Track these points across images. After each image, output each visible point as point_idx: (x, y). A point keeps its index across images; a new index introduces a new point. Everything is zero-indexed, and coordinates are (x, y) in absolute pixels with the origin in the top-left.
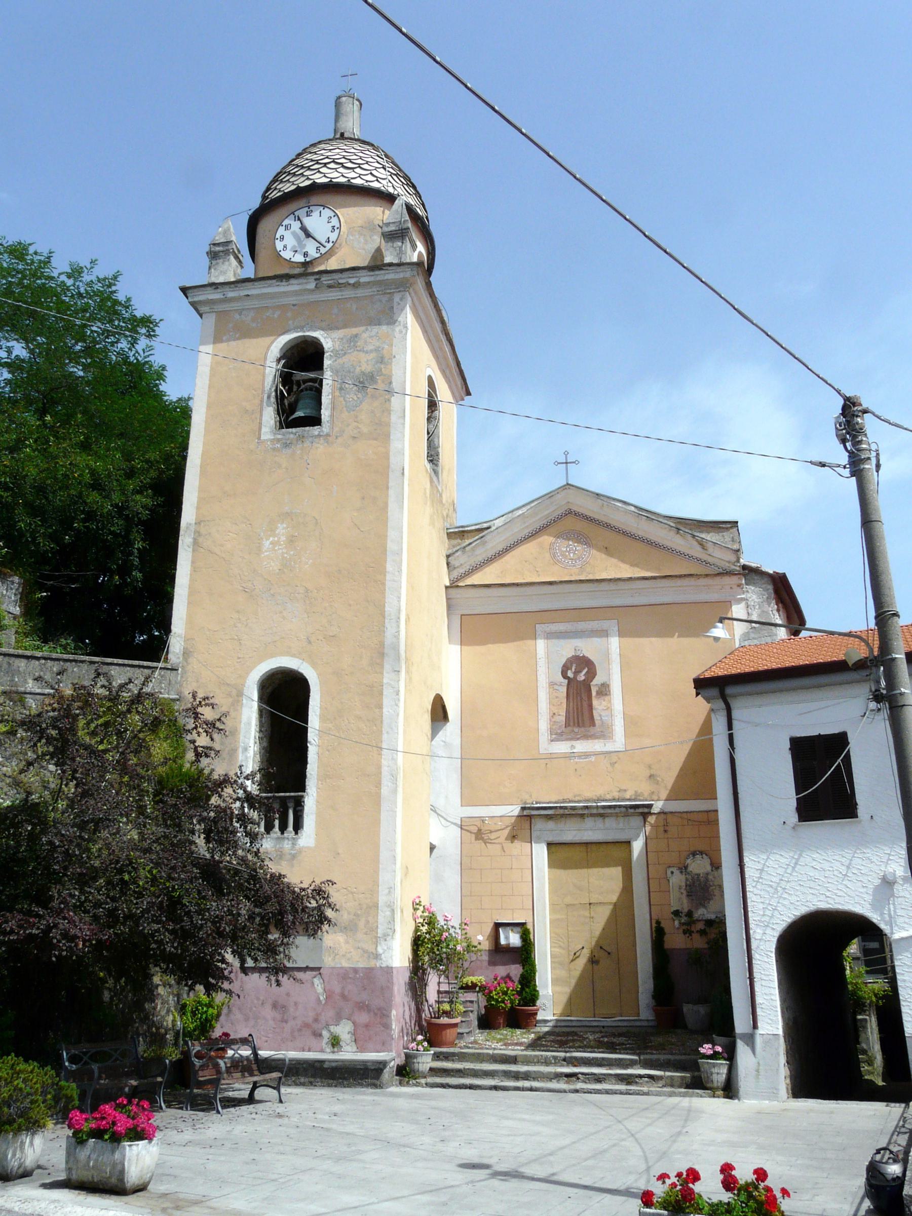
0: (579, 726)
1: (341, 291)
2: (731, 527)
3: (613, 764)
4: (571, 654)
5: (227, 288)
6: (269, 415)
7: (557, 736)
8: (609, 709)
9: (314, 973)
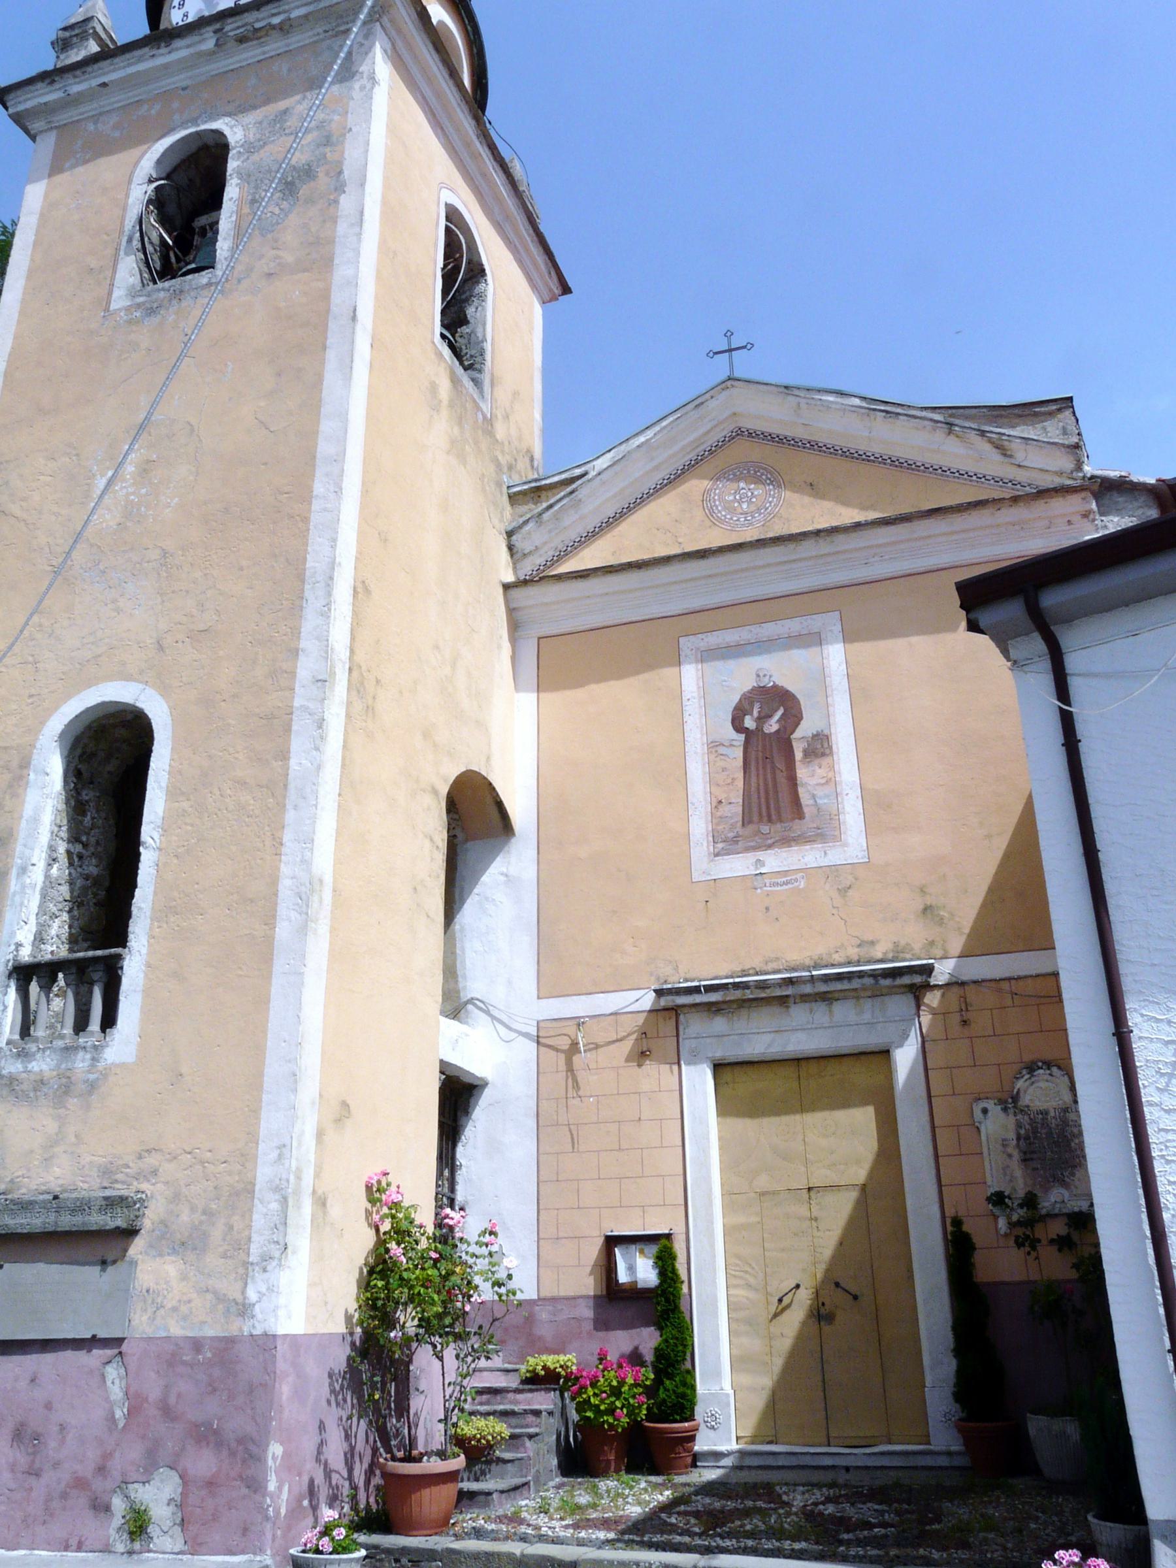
0: (770, 820)
1: (261, 45)
2: (1059, 410)
3: (844, 891)
4: (749, 684)
5: (69, 79)
6: (129, 270)
7: (727, 843)
8: (831, 782)
9: (109, 1352)
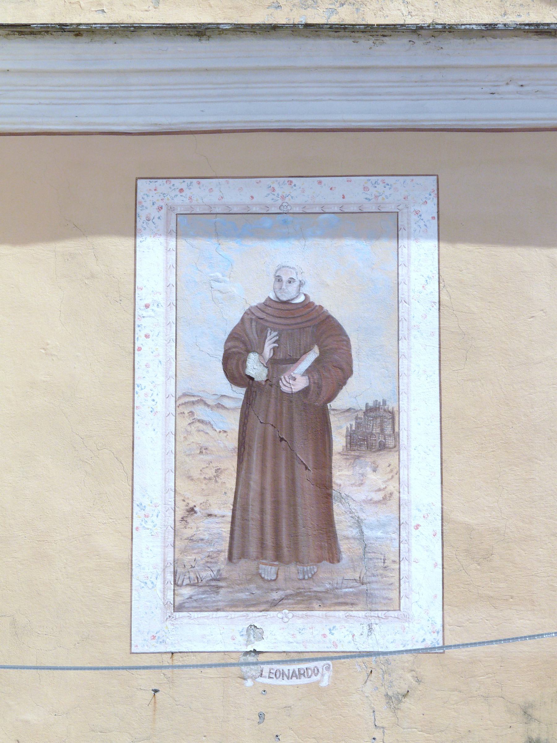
0: (278, 557)
3: (395, 700)
4: (260, 293)
7: (196, 590)
